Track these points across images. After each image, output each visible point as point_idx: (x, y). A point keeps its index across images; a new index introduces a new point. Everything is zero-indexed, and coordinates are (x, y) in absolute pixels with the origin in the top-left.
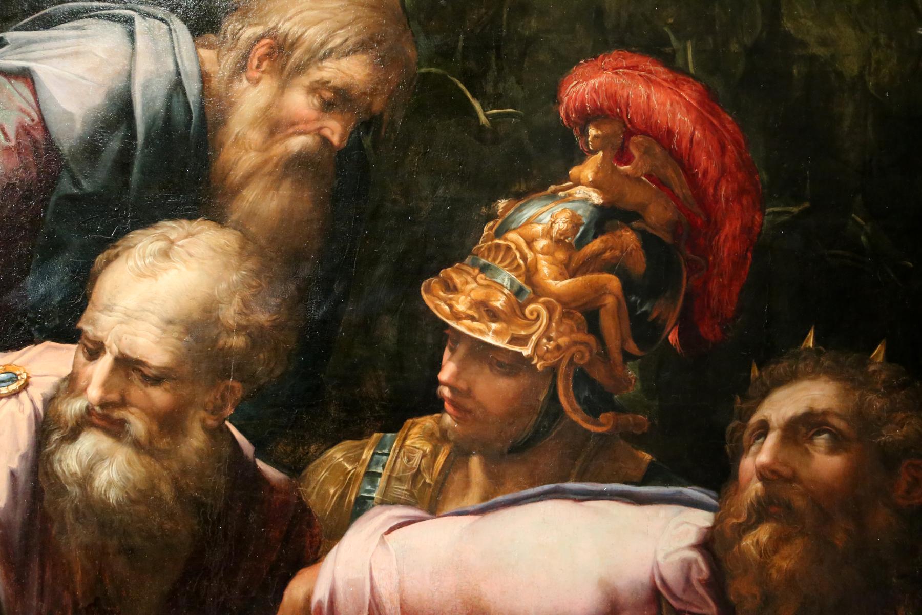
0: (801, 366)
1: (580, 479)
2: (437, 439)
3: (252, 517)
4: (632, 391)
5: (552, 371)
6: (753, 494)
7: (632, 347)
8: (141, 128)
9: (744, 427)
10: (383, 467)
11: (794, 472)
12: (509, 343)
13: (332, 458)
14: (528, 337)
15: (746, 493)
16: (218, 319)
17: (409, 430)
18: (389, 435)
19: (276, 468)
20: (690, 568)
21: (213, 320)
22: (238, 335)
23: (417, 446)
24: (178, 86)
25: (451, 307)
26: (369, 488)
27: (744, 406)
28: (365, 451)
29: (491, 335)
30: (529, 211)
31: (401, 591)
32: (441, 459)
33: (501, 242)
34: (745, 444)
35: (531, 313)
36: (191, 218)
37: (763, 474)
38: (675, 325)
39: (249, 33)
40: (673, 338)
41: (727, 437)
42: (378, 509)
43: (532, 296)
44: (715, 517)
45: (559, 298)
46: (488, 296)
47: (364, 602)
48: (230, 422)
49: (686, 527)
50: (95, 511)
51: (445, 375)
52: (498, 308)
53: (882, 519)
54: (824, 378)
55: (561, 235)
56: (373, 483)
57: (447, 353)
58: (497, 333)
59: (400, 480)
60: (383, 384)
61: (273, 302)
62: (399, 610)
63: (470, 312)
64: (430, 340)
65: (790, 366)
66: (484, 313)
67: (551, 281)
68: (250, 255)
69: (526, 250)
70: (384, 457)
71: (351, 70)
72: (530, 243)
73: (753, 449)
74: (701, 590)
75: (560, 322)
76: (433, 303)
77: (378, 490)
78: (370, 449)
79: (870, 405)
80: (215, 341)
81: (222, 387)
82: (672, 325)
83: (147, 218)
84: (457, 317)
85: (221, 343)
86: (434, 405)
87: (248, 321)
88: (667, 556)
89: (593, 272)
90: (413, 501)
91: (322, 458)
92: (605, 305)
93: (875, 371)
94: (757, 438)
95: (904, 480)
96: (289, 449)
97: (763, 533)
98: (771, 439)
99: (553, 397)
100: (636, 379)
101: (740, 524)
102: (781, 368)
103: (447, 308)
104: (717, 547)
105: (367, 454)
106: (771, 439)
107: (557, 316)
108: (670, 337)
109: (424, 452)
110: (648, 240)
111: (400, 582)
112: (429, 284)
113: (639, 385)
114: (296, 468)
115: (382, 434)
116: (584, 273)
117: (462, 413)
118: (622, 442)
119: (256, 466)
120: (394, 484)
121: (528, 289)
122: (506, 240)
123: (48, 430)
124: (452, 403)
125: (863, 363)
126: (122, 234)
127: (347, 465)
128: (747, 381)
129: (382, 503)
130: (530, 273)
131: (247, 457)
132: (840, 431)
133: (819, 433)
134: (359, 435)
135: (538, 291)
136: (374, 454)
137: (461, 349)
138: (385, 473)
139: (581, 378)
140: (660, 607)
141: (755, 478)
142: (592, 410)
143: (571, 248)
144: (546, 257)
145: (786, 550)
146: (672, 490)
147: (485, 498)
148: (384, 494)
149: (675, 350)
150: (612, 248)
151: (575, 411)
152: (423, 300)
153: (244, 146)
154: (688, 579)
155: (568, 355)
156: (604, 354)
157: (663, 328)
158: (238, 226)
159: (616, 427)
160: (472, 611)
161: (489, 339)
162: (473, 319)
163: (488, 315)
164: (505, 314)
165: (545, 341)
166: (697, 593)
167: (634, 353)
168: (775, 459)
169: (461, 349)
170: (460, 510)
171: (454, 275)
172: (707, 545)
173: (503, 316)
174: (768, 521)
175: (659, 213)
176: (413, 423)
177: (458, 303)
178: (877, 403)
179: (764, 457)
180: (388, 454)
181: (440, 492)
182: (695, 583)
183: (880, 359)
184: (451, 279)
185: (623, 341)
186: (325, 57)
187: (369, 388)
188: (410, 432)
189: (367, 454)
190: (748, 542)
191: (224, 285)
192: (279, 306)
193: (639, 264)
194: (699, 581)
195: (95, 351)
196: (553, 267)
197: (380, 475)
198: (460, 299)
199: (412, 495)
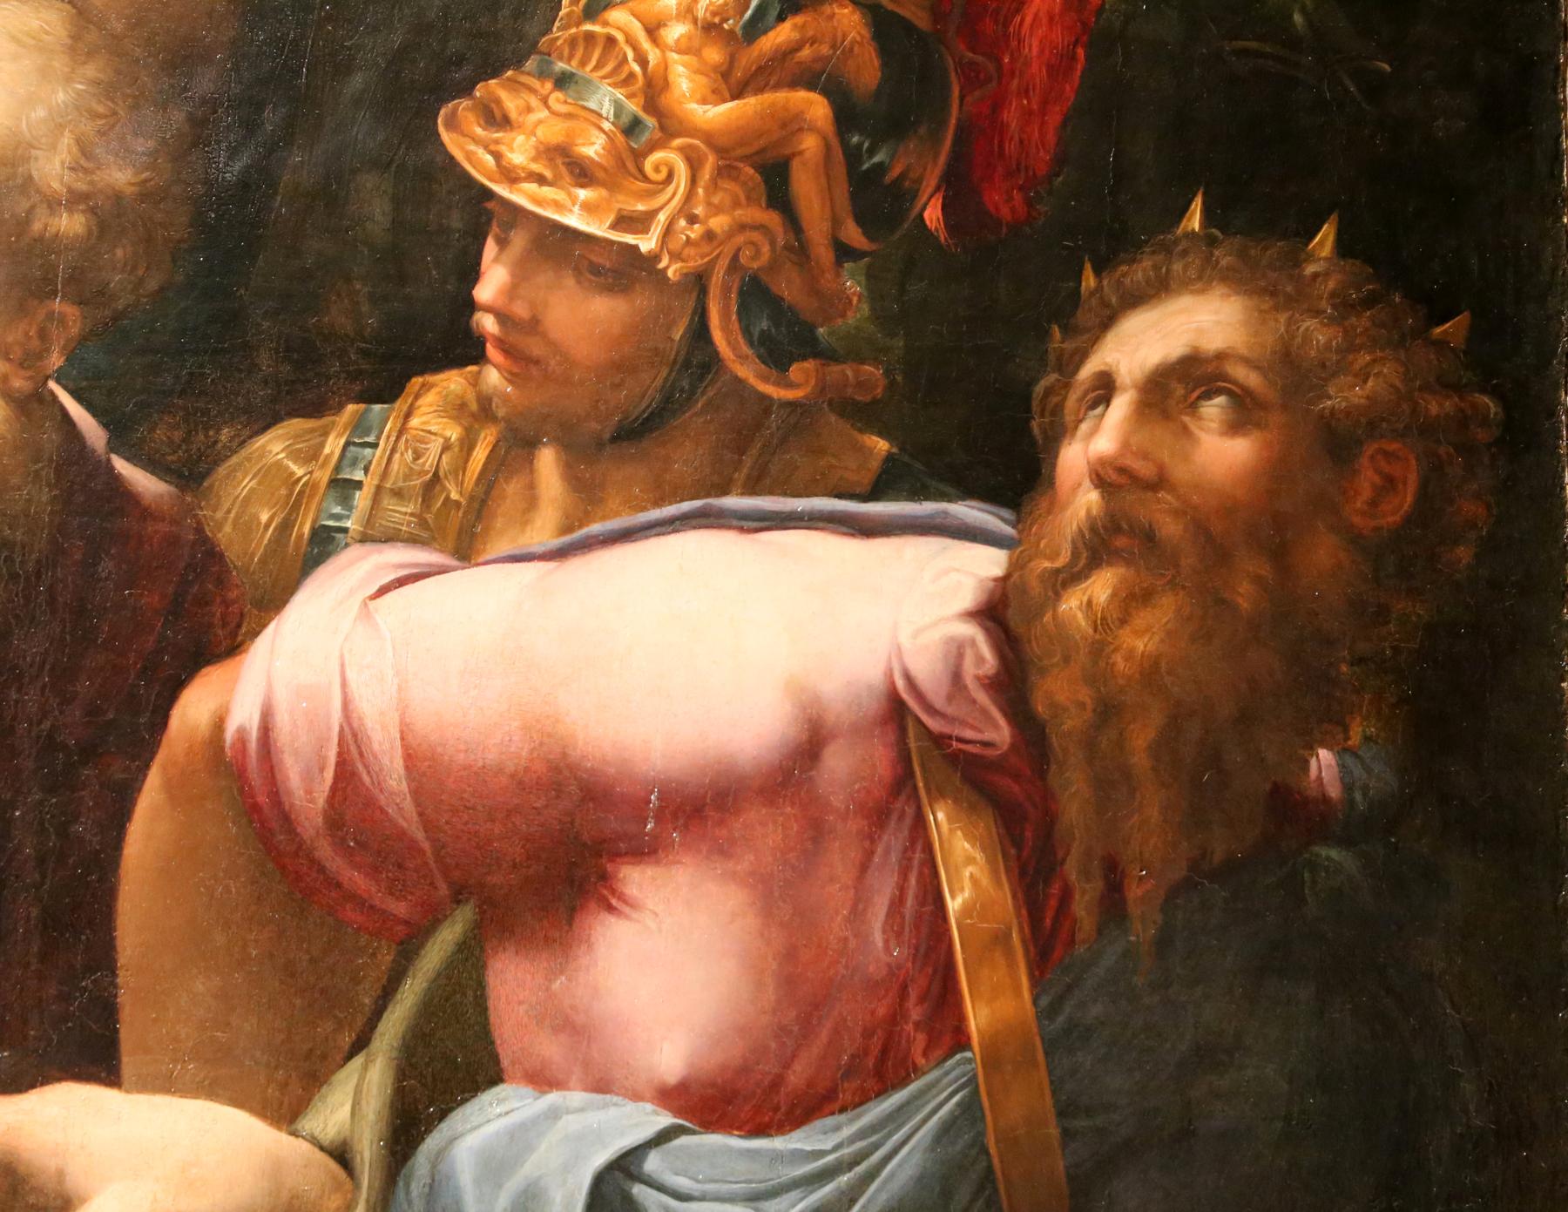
0: (1177, 267)
1: (752, 489)
2: (473, 415)
3: (106, 567)
4: (852, 319)
5: (698, 282)
6: (1083, 513)
7: (853, 234)
9: (1067, 386)
10: (366, 470)
11: (1161, 468)
12: (614, 227)
13: (263, 452)
14: (651, 215)
15: (1068, 513)
16: (30, 177)
17: (417, 397)
18: (377, 407)
19: (153, 473)
20: (960, 656)
21: (19, 181)
22: (70, 211)
23: (433, 428)
25: (498, 156)
26: (337, 510)
27: (1069, 346)
28: (331, 439)
29: (578, 212)
31: (403, 708)
32: (480, 455)
33: (596, 28)
34: (1069, 418)
35: (657, 169)
37: (1107, 477)
38: (938, 189)
40: (933, 215)
41: (1035, 404)
42: (355, 551)
43: (658, 135)
44: (1010, 558)
45: (709, 138)
46: (570, 134)
47: (329, 729)
48: (58, 381)
49: (954, 576)
51: (485, 292)
52: (589, 158)
53: (1323, 554)
54: (1219, 290)
55: (714, 14)
56: (346, 501)
57: (490, 249)
58: (588, 208)
59: (398, 494)
60: (365, 308)
61: (142, 145)
62: (398, 743)
63: (536, 167)
64: (456, 221)
65: (1156, 268)
66: (563, 169)
67: (694, 106)
68: (91, 54)
69: (646, 45)
70: (368, 451)
72: (652, 31)
73: (1084, 427)
74: (982, 698)
75: (714, 186)
76: (462, 149)
77: (356, 514)
78: (340, 435)
79: (1307, 338)
80: (25, 223)
81: (41, 315)
82: (930, 190)
85: (37, 227)
86: (468, 350)
87: (91, 183)
88: (917, 633)
89: (777, 87)
90: (425, 534)
91: (244, 453)
92: (801, 153)
93: (1315, 276)
94: (1093, 406)
95: (1367, 480)
96: (177, 435)
97: (1101, 587)
98: (1121, 406)
99: (700, 331)
100: (860, 296)
101: (1057, 571)
102: (1139, 271)
103: (489, 159)
104: (1013, 616)
105: (333, 446)
106: (1121, 406)
107: (706, 174)
108: (926, 214)
109: (447, 440)
111: (400, 689)
112: (454, 112)
113: (866, 308)
114: (191, 473)
115: (362, 406)
116: (760, 90)
118: (833, 418)
119: (113, 468)
120: (388, 502)
121: (650, 121)
122: (606, 24)
124: (501, 344)
125: (1295, 259)
127: (293, 467)
128: (1075, 294)
129: (364, 539)
130: (654, 90)
131: (94, 451)
132: (1247, 392)
133: (1208, 395)
134: (317, 408)
135: (670, 127)
136: (348, 444)
137: (519, 240)
138: (370, 483)
139: (755, 294)
140: (903, 730)
141: (1087, 483)
142: (776, 356)
144: (686, 58)
145: (1143, 618)
146: (927, 508)
147: (567, 529)
148: (369, 521)
149: (937, 238)
150: (813, 41)
151: (742, 358)
152: (442, 144)
154: (956, 677)
155: (728, 250)
156: (800, 250)
157: (915, 195)
159: (822, 389)
160: (541, 744)
161: (574, 220)
162: (541, 180)
163: (572, 173)
164: (605, 170)
165: (682, 223)
166: (974, 702)
167: (856, 245)
168: (1125, 445)
169: (519, 240)
170: (517, 552)
171: (503, 95)
172: (996, 612)
173: (600, 174)
174: (1110, 564)
176: (423, 385)
177: (512, 150)
178: (1319, 335)
180: (375, 446)
181: (479, 517)
182: (969, 681)
183: (1326, 251)
184: (498, 102)
185: (836, 223)
187: (337, 317)
188: (420, 402)
189: (333, 446)
190: (1071, 604)
191: (41, 113)
192: (154, 154)
193: (867, 71)
194: (978, 678)
196: (703, 80)
197: (359, 485)
198: (516, 141)
199: (423, 523)
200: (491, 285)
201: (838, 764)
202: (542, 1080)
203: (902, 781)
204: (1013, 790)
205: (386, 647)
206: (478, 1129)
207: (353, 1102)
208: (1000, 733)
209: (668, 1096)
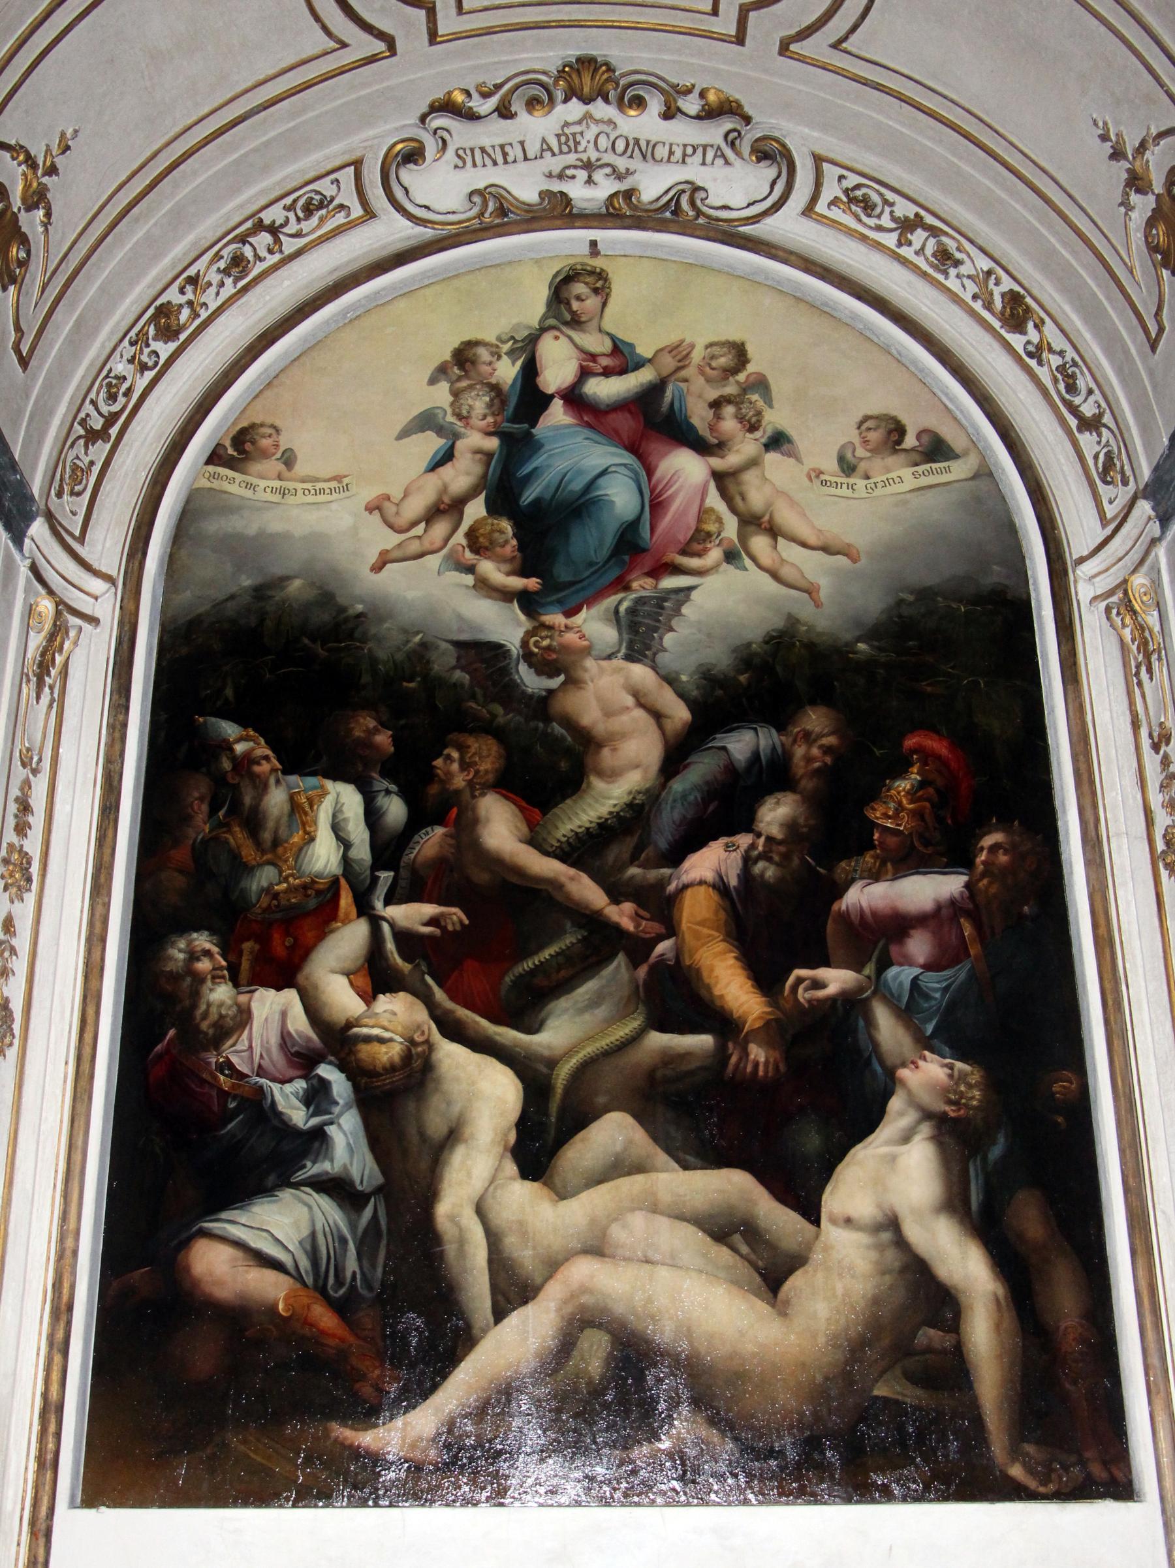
5: (911, 834)
8: (764, 763)
24: (774, 748)
30: (897, 784)
31: (870, 906)
36: (784, 790)
37: (983, 863)
39: (796, 730)
40: (949, 822)
45: (910, 810)
50: (765, 884)
71: (831, 740)
83: (770, 792)
84: (877, 818)
86: (873, 847)
97: (985, 881)
98: (985, 852)
99: (912, 842)
106: (985, 852)
110: (938, 791)
114: (830, 869)
117: (882, 849)
123: (748, 860)
126: (763, 797)
130: (900, 803)
134: (849, 858)
135: (903, 809)
139: (921, 836)
143: (912, 795)
153: (799, 766)
158: (800, 793)
172: (967, 886)
175: (940, 782)
178: (1017, 838)
179: (983, 858)
186: (823, 736)
195: (759, 835)
198: (877, 813)
200: (876, 836)
201: (944, 912)
202: (901, 965)
203: (955, 914)
204: (974, 916)
205: (864, 896)
206: (892, 971)
207: (869, 969)
208: (971, 906)
209: (922, 967)
